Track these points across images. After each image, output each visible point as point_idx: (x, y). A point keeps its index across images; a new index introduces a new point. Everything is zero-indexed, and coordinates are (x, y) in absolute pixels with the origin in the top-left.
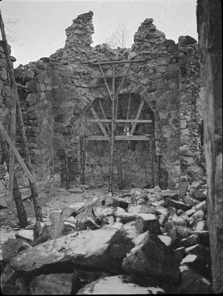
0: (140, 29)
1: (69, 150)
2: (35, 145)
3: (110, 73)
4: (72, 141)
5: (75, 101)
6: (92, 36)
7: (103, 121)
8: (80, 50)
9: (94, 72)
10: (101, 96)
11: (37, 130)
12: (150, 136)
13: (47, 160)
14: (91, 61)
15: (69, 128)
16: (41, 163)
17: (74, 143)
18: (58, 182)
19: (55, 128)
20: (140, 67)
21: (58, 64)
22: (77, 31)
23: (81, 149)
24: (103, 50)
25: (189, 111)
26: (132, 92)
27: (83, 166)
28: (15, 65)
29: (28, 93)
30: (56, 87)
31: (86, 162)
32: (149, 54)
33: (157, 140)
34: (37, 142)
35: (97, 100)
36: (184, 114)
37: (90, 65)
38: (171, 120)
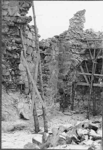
1: (66, 89)
2: (47, 85)
3: (93, 46)
4: (68, 84)
5: (71, 62)
7: (86, 74)
8: (77, 31)
9: (84, 45)
10: (86, 59)
11: (49, 77)
13: (53, 94)
14: (83, 39)
15: (67, 77)
16: (49, 96)
17: (69, 86)
19: (59, 76)
21: (64, 39)
22: (76, 21)
23: (73, 89)
24: (90, 33)
27: (73, 99)
28: (40, 39)
29: (46, 55)
30: (62, 53)
31: (75, 98)
34: (48, 83)
35: (84, 62)
37: (82, 41)
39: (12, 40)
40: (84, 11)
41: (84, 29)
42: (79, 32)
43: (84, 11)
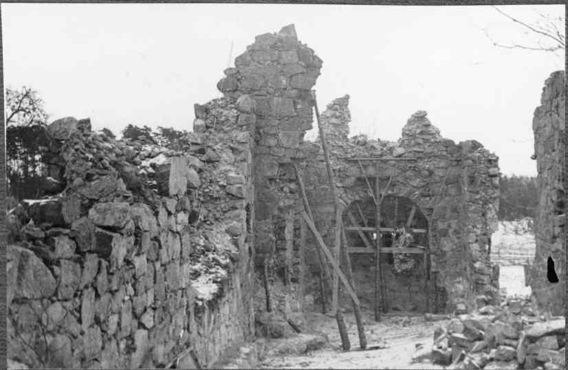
0: (410, 122)
3: (371, 171)
6: (349, 124)
7: (364, 229)
8: (337, 142)
9: (352, 168)
10: (357, 198)
12: (424, 249)
14: (349, 156)
18: (311, 305)
20: (409, 165)
22: (334, 120)
24: (363, 143)
25: (479, 224)
26: (401, 195)
30: (311, 188)
32: (422, 152)
33: (433, 253)
36: (473, 227)
37: (347, 160)
38: (451, 231)
39: (282, 189)
40: (347, 98)
41: (349, 136)
42: (341, 144)
43: (347, 98)
